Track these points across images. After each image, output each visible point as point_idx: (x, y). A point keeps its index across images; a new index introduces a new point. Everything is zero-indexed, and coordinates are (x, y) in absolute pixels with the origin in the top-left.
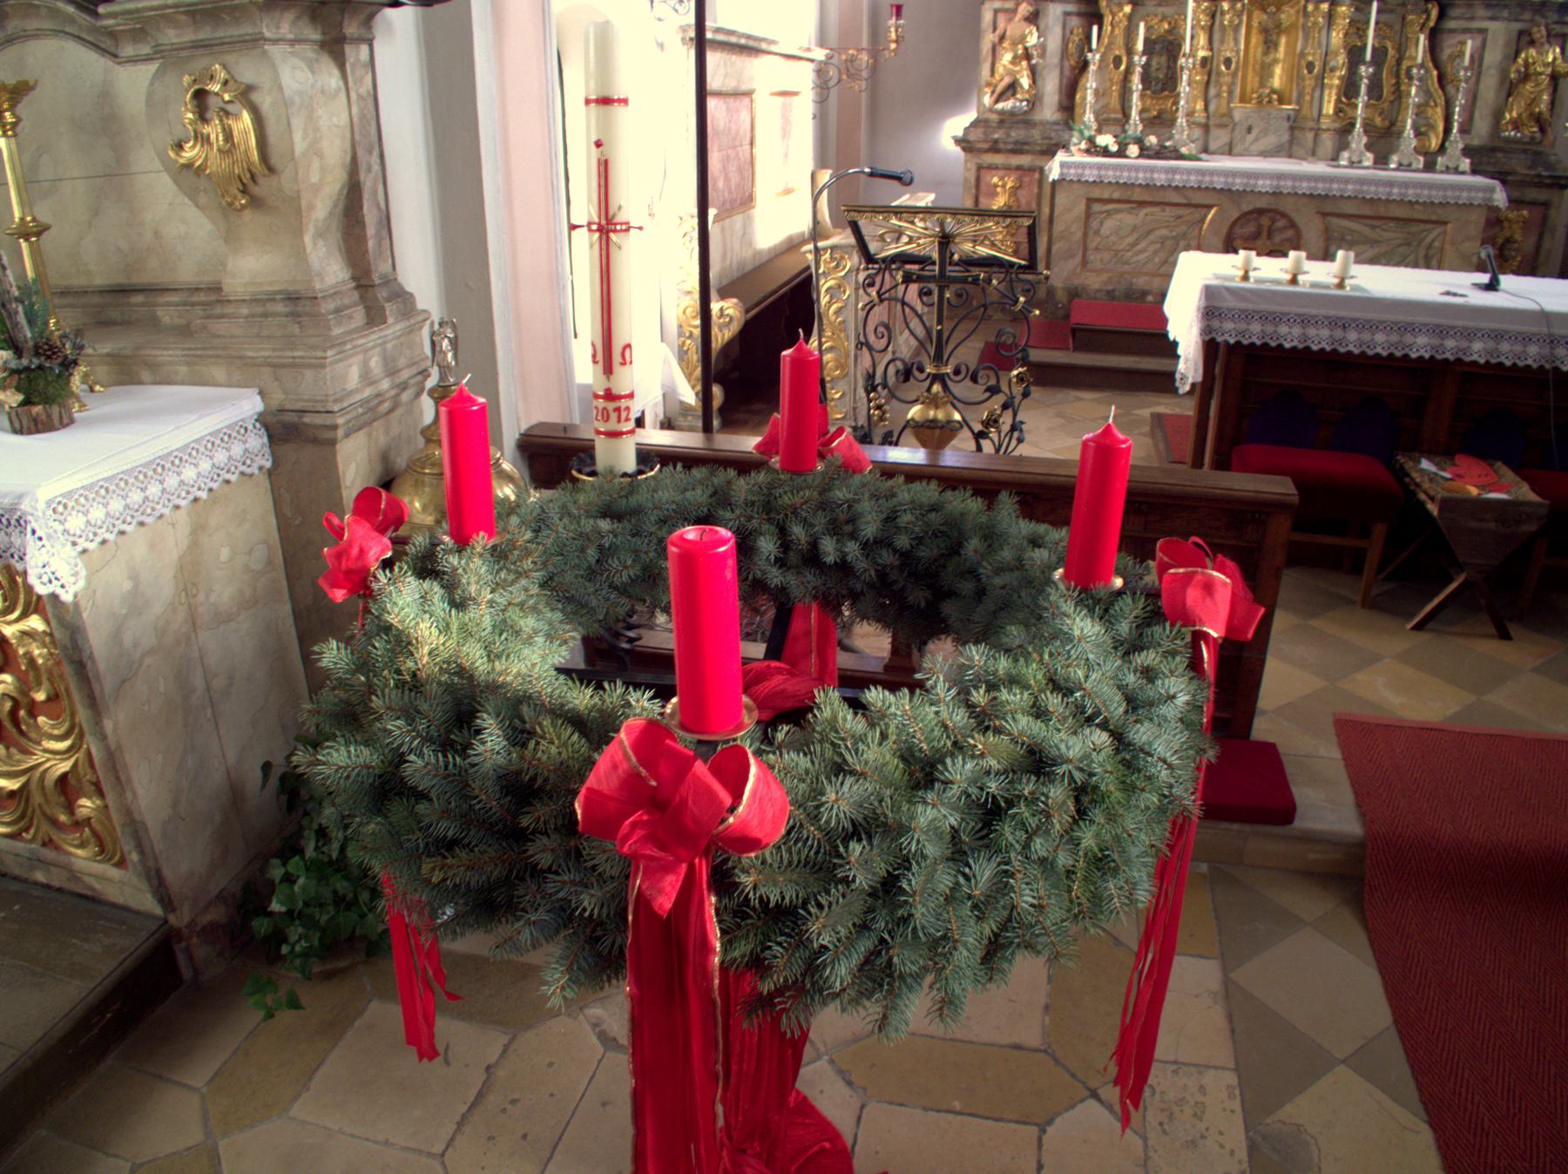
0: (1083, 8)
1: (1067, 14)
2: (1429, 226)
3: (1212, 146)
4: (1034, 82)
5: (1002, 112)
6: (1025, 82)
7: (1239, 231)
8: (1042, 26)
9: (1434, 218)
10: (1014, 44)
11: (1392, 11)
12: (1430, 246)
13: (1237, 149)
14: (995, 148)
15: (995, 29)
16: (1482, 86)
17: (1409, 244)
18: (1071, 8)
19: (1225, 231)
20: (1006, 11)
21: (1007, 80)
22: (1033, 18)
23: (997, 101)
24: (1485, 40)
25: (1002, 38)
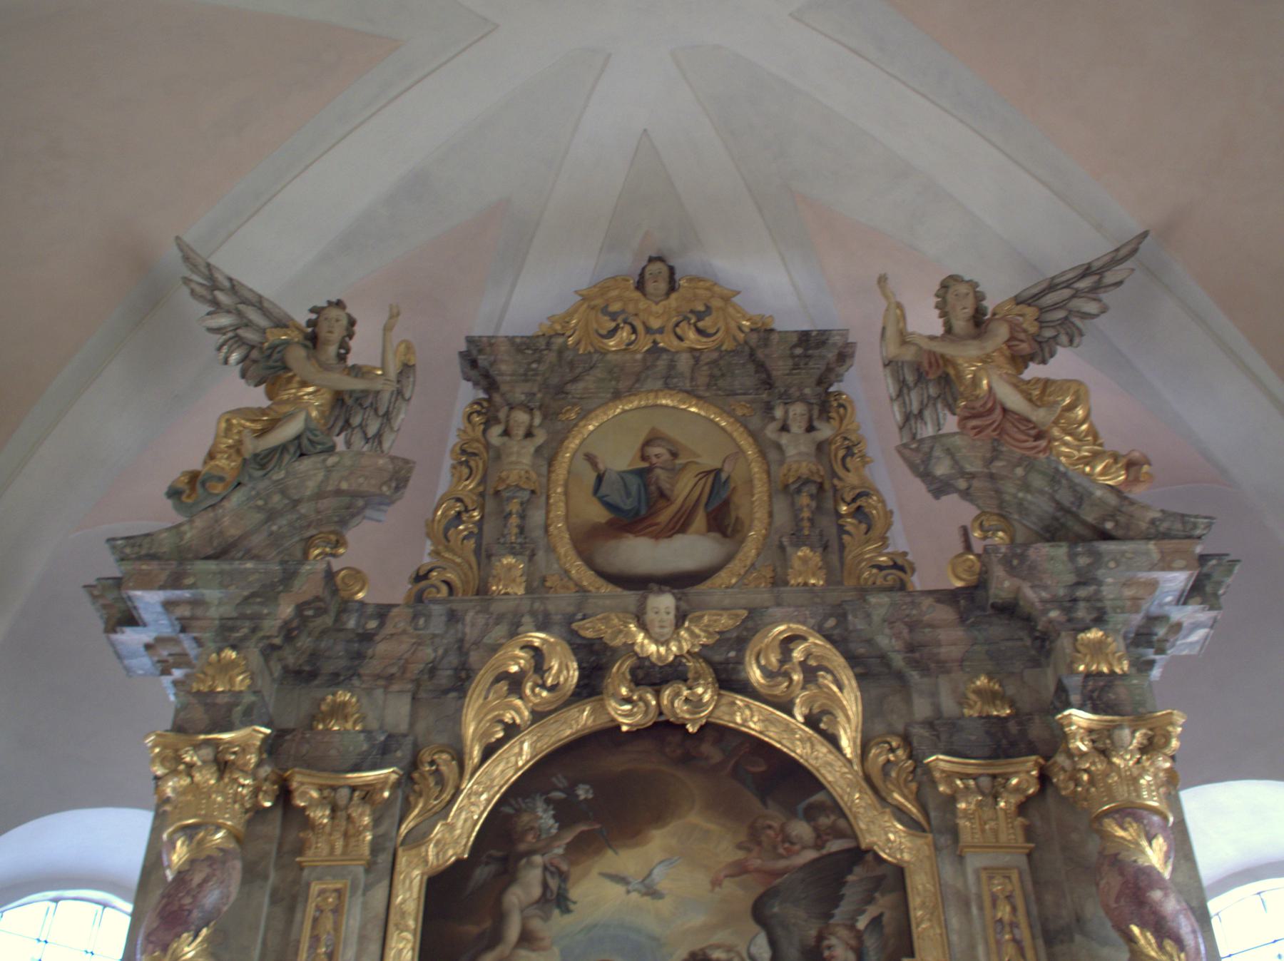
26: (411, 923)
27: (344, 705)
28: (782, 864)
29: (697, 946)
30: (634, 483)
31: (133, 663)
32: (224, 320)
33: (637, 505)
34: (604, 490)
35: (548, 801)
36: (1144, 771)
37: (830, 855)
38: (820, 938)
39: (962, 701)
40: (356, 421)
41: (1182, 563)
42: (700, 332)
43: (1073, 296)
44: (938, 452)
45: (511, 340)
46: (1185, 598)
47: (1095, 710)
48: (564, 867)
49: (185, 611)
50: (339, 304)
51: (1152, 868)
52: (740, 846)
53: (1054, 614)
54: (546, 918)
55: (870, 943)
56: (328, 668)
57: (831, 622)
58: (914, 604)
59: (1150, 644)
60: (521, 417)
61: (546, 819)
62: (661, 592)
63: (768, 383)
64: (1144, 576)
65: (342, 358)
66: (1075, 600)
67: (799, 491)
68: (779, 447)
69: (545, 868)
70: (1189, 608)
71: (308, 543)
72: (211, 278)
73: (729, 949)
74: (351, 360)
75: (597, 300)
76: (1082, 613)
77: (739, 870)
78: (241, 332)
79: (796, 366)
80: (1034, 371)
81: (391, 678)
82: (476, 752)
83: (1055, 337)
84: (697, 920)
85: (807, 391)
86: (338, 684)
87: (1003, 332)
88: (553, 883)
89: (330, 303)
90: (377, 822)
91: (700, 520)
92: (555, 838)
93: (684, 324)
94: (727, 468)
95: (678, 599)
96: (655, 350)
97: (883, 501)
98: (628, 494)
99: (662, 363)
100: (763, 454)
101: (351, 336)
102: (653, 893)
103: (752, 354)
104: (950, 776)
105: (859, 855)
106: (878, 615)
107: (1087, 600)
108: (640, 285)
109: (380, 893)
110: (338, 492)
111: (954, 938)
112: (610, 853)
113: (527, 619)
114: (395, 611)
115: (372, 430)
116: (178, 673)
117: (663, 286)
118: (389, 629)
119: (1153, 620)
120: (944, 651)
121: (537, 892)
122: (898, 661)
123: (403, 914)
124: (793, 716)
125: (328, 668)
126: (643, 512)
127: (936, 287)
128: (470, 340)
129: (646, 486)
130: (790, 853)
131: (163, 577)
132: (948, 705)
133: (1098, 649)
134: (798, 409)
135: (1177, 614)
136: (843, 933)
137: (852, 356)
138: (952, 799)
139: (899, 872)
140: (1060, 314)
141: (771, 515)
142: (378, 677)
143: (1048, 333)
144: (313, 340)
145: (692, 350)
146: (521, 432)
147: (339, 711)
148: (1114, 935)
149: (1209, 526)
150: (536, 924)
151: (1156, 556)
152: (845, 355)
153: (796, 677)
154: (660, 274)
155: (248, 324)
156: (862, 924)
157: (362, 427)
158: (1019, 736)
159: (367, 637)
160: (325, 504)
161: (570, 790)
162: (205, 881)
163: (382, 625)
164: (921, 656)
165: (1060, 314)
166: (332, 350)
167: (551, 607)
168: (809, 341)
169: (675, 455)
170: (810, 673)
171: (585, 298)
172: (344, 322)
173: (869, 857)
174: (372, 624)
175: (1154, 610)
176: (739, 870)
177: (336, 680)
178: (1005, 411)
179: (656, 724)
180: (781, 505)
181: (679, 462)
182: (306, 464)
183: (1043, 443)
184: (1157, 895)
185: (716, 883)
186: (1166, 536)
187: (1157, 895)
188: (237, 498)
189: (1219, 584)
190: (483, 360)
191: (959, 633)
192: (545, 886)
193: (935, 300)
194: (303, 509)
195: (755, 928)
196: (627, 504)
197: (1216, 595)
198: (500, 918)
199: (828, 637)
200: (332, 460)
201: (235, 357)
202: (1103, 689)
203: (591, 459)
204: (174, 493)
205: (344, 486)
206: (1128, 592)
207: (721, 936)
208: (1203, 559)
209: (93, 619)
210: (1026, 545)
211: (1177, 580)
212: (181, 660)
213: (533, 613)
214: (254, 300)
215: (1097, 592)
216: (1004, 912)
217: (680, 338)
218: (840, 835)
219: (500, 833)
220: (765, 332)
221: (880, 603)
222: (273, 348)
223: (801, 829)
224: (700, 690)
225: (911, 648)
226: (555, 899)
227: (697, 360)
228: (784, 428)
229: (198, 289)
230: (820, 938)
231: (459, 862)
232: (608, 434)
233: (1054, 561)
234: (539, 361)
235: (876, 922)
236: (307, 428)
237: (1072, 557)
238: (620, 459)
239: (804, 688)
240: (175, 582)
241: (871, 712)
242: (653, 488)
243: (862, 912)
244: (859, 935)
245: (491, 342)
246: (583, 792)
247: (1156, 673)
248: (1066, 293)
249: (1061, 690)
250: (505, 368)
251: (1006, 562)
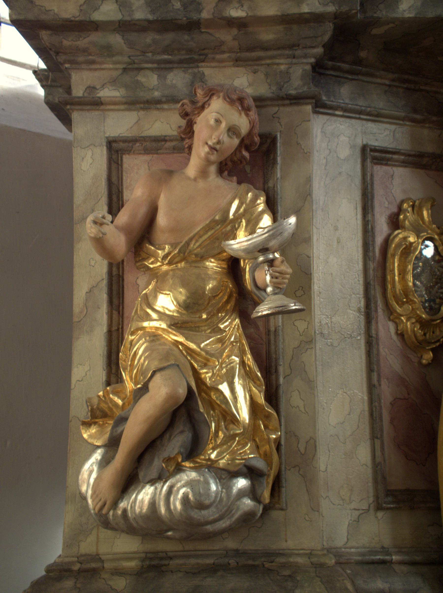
1: (373, 156)
4: (272, 397)
5: (152, 525)
6: (240, 398)
8: (287, 192)
10: (188, 256)
15: (115, 204)
18: (383, 135)
20: (154, 145)
21: (162, 391)
22: (253, 162)
23: (129, 482)
25: (143, 236)
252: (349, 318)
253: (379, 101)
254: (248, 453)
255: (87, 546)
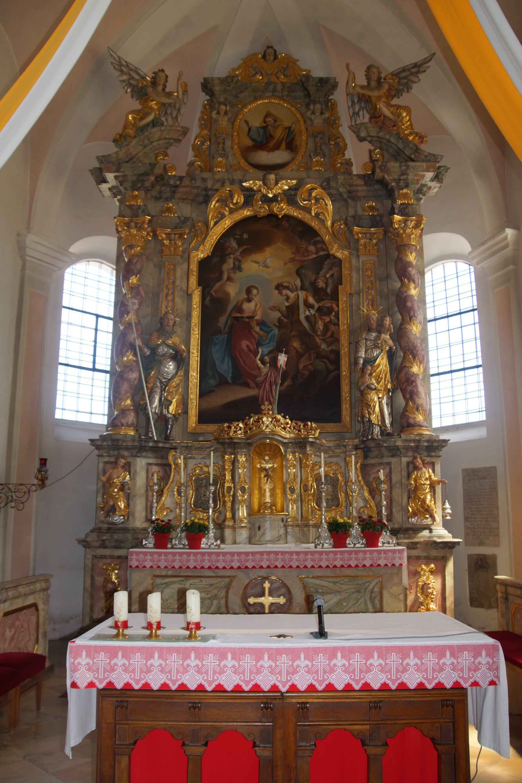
0: (159, 461)
2: (368, 579)
3: (238, 541)
6: (122, 505)
7: (250, 591)
9: (371, 573)
11: (338, 456)
12: (372, 592)
13: (253, 541)
14: (103, 545)
16: (394, 494)
17: (359, 592)
18: (151, 461)
19: (241, 592)
20: (111, 463)
24: (391, 469)
26: (195, 274)
27: (170, 208)
28: (306, 258)
29: (279, 282)
30: (261, 131)
31: (105, 193)
32: (125, 77)
33: (263, 140)
34: (251, 134)
35: (235, 239)
36: (413, 233)
37: (320, 256)
38: (316, 280)
39: (364, 210)
40: (169, 112)
41: (432, 170)
42: (284, 75)
43: (410, 74)
44: (362, 129)
45: (219, 79)
46: (432, 180)
47: (401, 216)
48: (240, 259)
49: (121, 179)
50: (163, 71)
51: (410, 262)
52: (293, 253)
53: (393, 184)
54: (235, 273)
55: (330, 281)
56: (165, 196)
57: (325, 184)
58: (351, 179)
59: (421, 193)
60: (223, 107)
61: (234, 244)
62: (271, 173)
63: (308, 95)
64: (421, 173)
65: (164, 90)
66: (400, 180)
67: (317, 136)
68: (311, 120)
69: (234, 259)
70: (434, 183)
71: (157, 156)
72: (120, 62)
73: (289, 283)
74: (167, 90)
75: (249, 63)
76: (402, 184)
77: (292, 260)
78: (131, 81)
79: (318, 90)
80: (395, 101)
81: (184, 199)
82: (212, 223)
83: (403, 89)
84: (280, 274)
85: (321, 99)
86: (168, 201)
87: (386, 87)
88: (237, 263)
89: (159, 70)
90: (183, 244)
91: (283, 146)
92: (237, 250)
93: (279, 73)
94: (293, 126)
95: (276, 175)
96: (269, 83)
97: (344, 141)
98: (259, 136)
99: (271, 87)
100: (305, 122)
101: (166, 81)
102: (266, 266)
103: (303, 84)
104: (358, 233)
105: (329, 256)
106: (340, 182)
107: (404, 180)
108: (264, 57)
109: (185, 266)
110: (165, 139)
111: (354, 280)
112: (254, 255)
113: (227, 181)
114: (185, 178)
115: (174, 115)
116: (119, 197)
117: (272, 58)
118: (183, 184)
119: (423, 186)
120: (360, 194)
121: (232, 266)
122: (345, 196)
123: (193, 271)
124: (310, 213)
125: (165, 196)
126: (264, 142)
127: (365, 68)
128: (205, 79)
129: (265, 132)
130: (308, 255)
131: (114, 168)
132: (360, 212)
133: (405, 196)
134: (318, 106)
135: (430, 184)
136: (323, 278)
137: (337, 86)
138: (358, 240)
139: (340, 261)
140: (405, 81)
141: (307, 144)
142: (180, 199)
143: (401, 87)
144: (154, 83)
145: (282, 83)
146: (222, 113)
147: (169, 210)
148: (398, 279)
149: (441, 159)
150: (232, 275)
151: (425, 167)
152: (335, 86)
153: (313, 201)
154: (269, 53)
155: (133, 78)
156: (328, 276)
157: (171, 114)
158: (381, 221)
159: (176, 186)
160: (160, 142)
161: (241, 235)
162: (137, 262)
163: (181, 183)
164: (352, 195)
165: (405, 81)
166: (160, 88)
167: (235, 177)
168: (323, 82)
169: (275, 121)
170: (317, 200)
171: (244, 62)
172: (164, 77)
173: (332, 257)
174: (178, 183)
175: (423, 182)
176: (292, 260)
177: (167, 200)
178: (385, 116)
179: (268, 215)
180: (311, 141)
181: (277, 124)
182: (155, 130)
183: (395, 128)
184: (410, 269)
185: (285, 264)
186: (429, 161)
187: (410, 269)
188: (134, 142)
189: (443, 175)
190: (209, 86)
191: (365, 188)
192: (234, 264)
193: (365, 73)
194: (154, 144)
195: (297, 277)
196: (259, 139)
197: (442, 179)
198: (221, 273)
199: (323, 189)
200: (163, 128)
201: (129, 90)
202: (405, 208)
203: (247, 122)
204: (115, 141)
205: (167, 137)
206: (416, 178)
207: (286, 279)
208: (439, 167)
209: (92, 180)
210: (387, 162)
211: (430, 175)
212: (120, 193)
213: (229, 180)
214: (134, 69)
215: (407, 178)
216: (369, 273)
217: (278, 78)
218: (323, 250)
219: (220, 248)
220: (308, 77)
221: (341, 178)
222: (142, 88)
223: (312, 248)
224: (282, 205)
225: (349, 192)
226: (238, 268)
227: (284, 86)
228: (313, 113)
229: (116, 66)
230: (316, 280)
231: (208, 256)
232: (253, 113)
233: (394, 166)
234: (229, 86)
235: (332, 276)
236: (155, 117)
237: (400, 167)
238: (256, 123)
239: (315, 205)
240: (118, 171)
241: (336, 211)
242: (268, 133)
243: (328, 272)
244: (327, 279)
245: (212, 79)
246: (245, 236)
247: (422, 201)
248: (408, 73)
249: (393, 208)
250: (217, 89)
251: (380, 167)
252: (143, 491)
253: (150, 455)
254: (123, 513)
255: (100, 525)
